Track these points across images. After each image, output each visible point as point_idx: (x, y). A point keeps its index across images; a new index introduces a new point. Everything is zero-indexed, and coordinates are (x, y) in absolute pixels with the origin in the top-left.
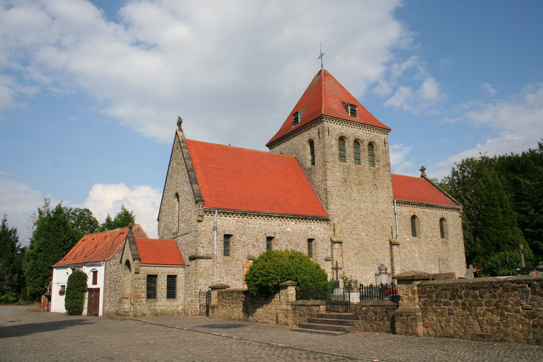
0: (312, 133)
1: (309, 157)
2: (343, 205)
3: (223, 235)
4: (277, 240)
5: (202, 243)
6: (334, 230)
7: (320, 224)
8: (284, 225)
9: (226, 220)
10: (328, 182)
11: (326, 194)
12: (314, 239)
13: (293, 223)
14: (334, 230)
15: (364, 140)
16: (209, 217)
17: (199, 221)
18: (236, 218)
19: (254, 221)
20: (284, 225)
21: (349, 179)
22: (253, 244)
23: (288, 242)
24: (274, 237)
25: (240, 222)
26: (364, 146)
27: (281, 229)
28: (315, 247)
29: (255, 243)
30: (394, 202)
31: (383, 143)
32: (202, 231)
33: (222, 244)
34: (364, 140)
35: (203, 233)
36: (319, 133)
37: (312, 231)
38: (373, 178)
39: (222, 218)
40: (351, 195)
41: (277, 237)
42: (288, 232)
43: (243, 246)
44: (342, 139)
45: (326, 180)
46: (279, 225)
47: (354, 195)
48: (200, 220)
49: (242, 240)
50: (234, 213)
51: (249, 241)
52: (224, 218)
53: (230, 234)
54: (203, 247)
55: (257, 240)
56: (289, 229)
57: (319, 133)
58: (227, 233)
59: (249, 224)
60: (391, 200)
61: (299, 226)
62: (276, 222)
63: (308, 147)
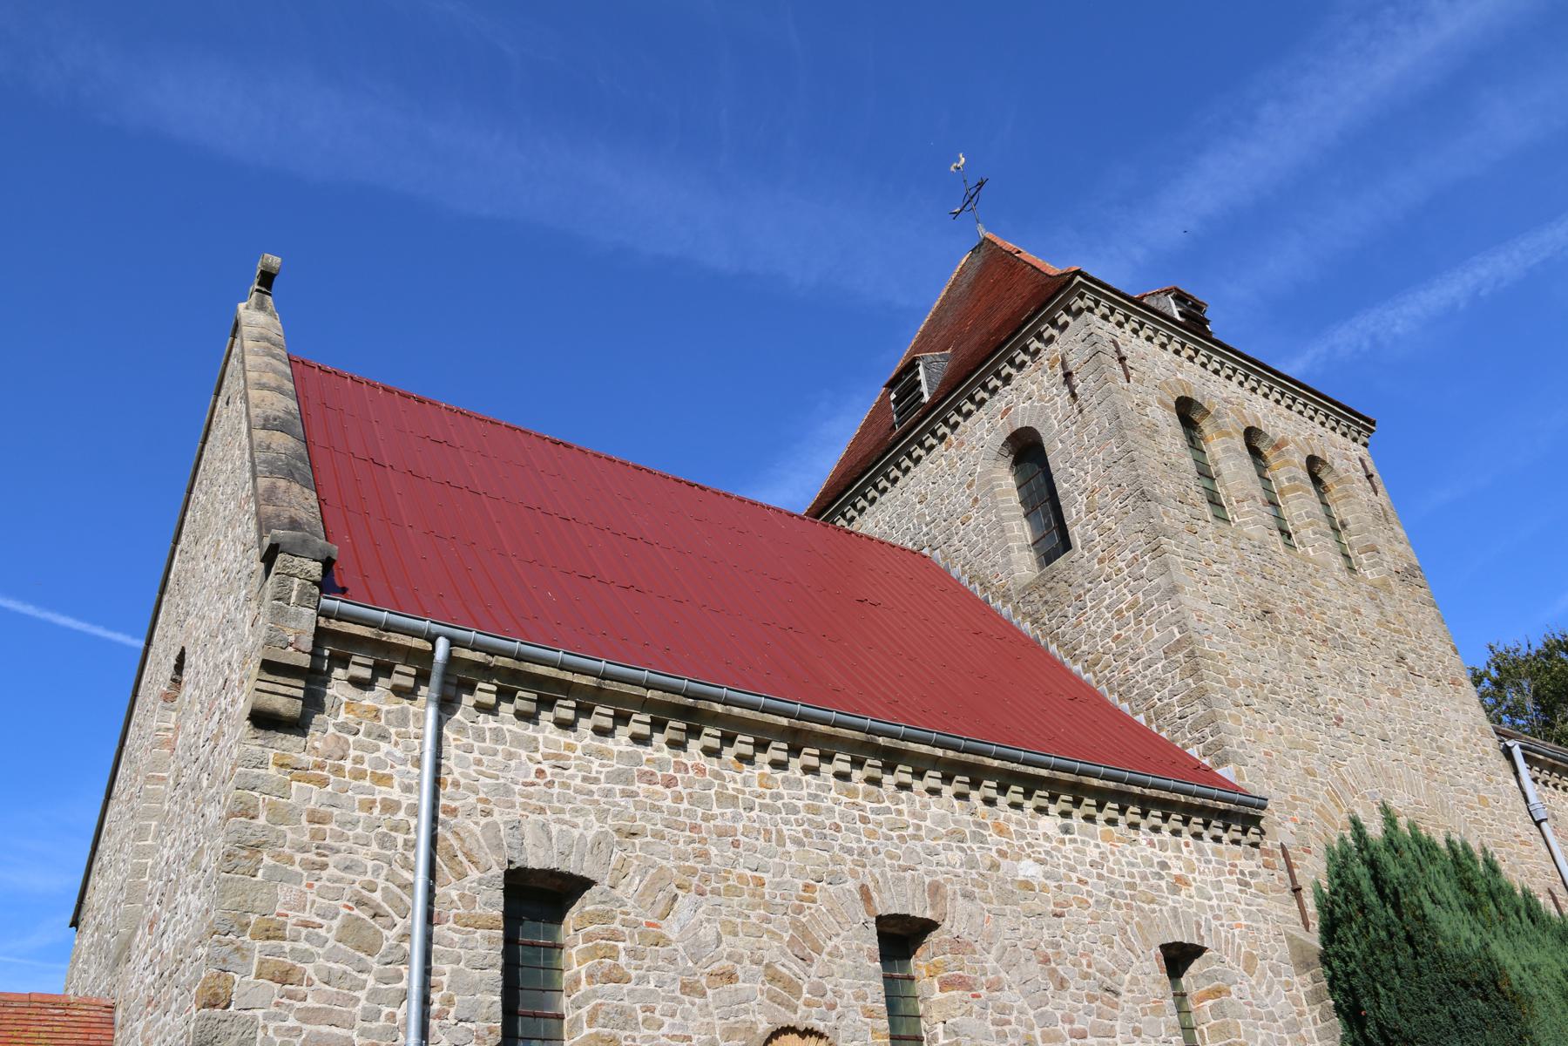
0: (1027, 395)
1: (1021, 531)
2: (1294, 745)
3: (498, 871)
4: (958, 945)
5: (272, 932)
6: (1296, 890)
7: (1208, 844)
8: (992, 836)
9: (532, 745)
10: (1187, 598)
11: (1195, 671)
12: (1198, 951)
13: (1050, 824)
14: (1296, 890)
15: (1284, 442)
16: (368, 699)
17: (263, 720)
18: (621, 741)
19: (765, 782)
20: (992, 836)
21: (1283, 609)
22: (774, 978)
23: (1035, 967)
24: (929, 926)
25: (649, 778)
26: (1288, 471)
27: (971, 863)
28: (1219, 1011)
29: (790, 968)
30: (1508, 753)
31: (1362, 475)
32: (280, 816)
33: (488, 946)
34: (1284, 442)
35: (297, 833)
36: (1068, 376)
37: (1174, 890)
38: (1380, 623)
39: (487, 722)
40: (1314, 693)
41: (956, 921)
42: (1027, 885)
43: (688, 988)
44: (1187, 412)
45: (1174, 590)
46: (957, 836)
47: (1329, 691)
48: (280, 705)
49: (671, 928)
50: (599, 695)
51: (742, 944)
52: (519, 728)
53: (572, 866)
54: (284, 977)
55: (805, 946)
56: (1028, 869)
57: (1068, 376)
58: (536, 859)
59: (723, 799)
60: (1491, 744)
61: (1093, 853)
62: (935, 807)
63: (1007, 481)
